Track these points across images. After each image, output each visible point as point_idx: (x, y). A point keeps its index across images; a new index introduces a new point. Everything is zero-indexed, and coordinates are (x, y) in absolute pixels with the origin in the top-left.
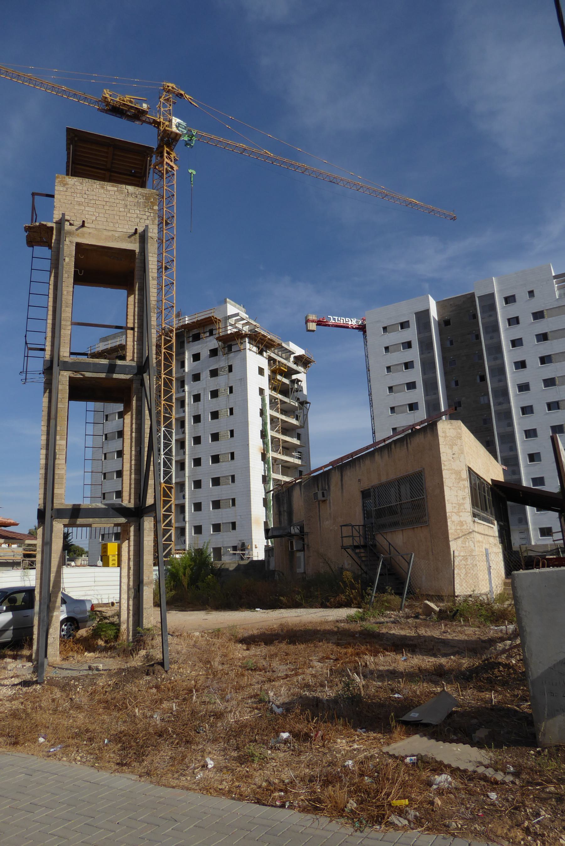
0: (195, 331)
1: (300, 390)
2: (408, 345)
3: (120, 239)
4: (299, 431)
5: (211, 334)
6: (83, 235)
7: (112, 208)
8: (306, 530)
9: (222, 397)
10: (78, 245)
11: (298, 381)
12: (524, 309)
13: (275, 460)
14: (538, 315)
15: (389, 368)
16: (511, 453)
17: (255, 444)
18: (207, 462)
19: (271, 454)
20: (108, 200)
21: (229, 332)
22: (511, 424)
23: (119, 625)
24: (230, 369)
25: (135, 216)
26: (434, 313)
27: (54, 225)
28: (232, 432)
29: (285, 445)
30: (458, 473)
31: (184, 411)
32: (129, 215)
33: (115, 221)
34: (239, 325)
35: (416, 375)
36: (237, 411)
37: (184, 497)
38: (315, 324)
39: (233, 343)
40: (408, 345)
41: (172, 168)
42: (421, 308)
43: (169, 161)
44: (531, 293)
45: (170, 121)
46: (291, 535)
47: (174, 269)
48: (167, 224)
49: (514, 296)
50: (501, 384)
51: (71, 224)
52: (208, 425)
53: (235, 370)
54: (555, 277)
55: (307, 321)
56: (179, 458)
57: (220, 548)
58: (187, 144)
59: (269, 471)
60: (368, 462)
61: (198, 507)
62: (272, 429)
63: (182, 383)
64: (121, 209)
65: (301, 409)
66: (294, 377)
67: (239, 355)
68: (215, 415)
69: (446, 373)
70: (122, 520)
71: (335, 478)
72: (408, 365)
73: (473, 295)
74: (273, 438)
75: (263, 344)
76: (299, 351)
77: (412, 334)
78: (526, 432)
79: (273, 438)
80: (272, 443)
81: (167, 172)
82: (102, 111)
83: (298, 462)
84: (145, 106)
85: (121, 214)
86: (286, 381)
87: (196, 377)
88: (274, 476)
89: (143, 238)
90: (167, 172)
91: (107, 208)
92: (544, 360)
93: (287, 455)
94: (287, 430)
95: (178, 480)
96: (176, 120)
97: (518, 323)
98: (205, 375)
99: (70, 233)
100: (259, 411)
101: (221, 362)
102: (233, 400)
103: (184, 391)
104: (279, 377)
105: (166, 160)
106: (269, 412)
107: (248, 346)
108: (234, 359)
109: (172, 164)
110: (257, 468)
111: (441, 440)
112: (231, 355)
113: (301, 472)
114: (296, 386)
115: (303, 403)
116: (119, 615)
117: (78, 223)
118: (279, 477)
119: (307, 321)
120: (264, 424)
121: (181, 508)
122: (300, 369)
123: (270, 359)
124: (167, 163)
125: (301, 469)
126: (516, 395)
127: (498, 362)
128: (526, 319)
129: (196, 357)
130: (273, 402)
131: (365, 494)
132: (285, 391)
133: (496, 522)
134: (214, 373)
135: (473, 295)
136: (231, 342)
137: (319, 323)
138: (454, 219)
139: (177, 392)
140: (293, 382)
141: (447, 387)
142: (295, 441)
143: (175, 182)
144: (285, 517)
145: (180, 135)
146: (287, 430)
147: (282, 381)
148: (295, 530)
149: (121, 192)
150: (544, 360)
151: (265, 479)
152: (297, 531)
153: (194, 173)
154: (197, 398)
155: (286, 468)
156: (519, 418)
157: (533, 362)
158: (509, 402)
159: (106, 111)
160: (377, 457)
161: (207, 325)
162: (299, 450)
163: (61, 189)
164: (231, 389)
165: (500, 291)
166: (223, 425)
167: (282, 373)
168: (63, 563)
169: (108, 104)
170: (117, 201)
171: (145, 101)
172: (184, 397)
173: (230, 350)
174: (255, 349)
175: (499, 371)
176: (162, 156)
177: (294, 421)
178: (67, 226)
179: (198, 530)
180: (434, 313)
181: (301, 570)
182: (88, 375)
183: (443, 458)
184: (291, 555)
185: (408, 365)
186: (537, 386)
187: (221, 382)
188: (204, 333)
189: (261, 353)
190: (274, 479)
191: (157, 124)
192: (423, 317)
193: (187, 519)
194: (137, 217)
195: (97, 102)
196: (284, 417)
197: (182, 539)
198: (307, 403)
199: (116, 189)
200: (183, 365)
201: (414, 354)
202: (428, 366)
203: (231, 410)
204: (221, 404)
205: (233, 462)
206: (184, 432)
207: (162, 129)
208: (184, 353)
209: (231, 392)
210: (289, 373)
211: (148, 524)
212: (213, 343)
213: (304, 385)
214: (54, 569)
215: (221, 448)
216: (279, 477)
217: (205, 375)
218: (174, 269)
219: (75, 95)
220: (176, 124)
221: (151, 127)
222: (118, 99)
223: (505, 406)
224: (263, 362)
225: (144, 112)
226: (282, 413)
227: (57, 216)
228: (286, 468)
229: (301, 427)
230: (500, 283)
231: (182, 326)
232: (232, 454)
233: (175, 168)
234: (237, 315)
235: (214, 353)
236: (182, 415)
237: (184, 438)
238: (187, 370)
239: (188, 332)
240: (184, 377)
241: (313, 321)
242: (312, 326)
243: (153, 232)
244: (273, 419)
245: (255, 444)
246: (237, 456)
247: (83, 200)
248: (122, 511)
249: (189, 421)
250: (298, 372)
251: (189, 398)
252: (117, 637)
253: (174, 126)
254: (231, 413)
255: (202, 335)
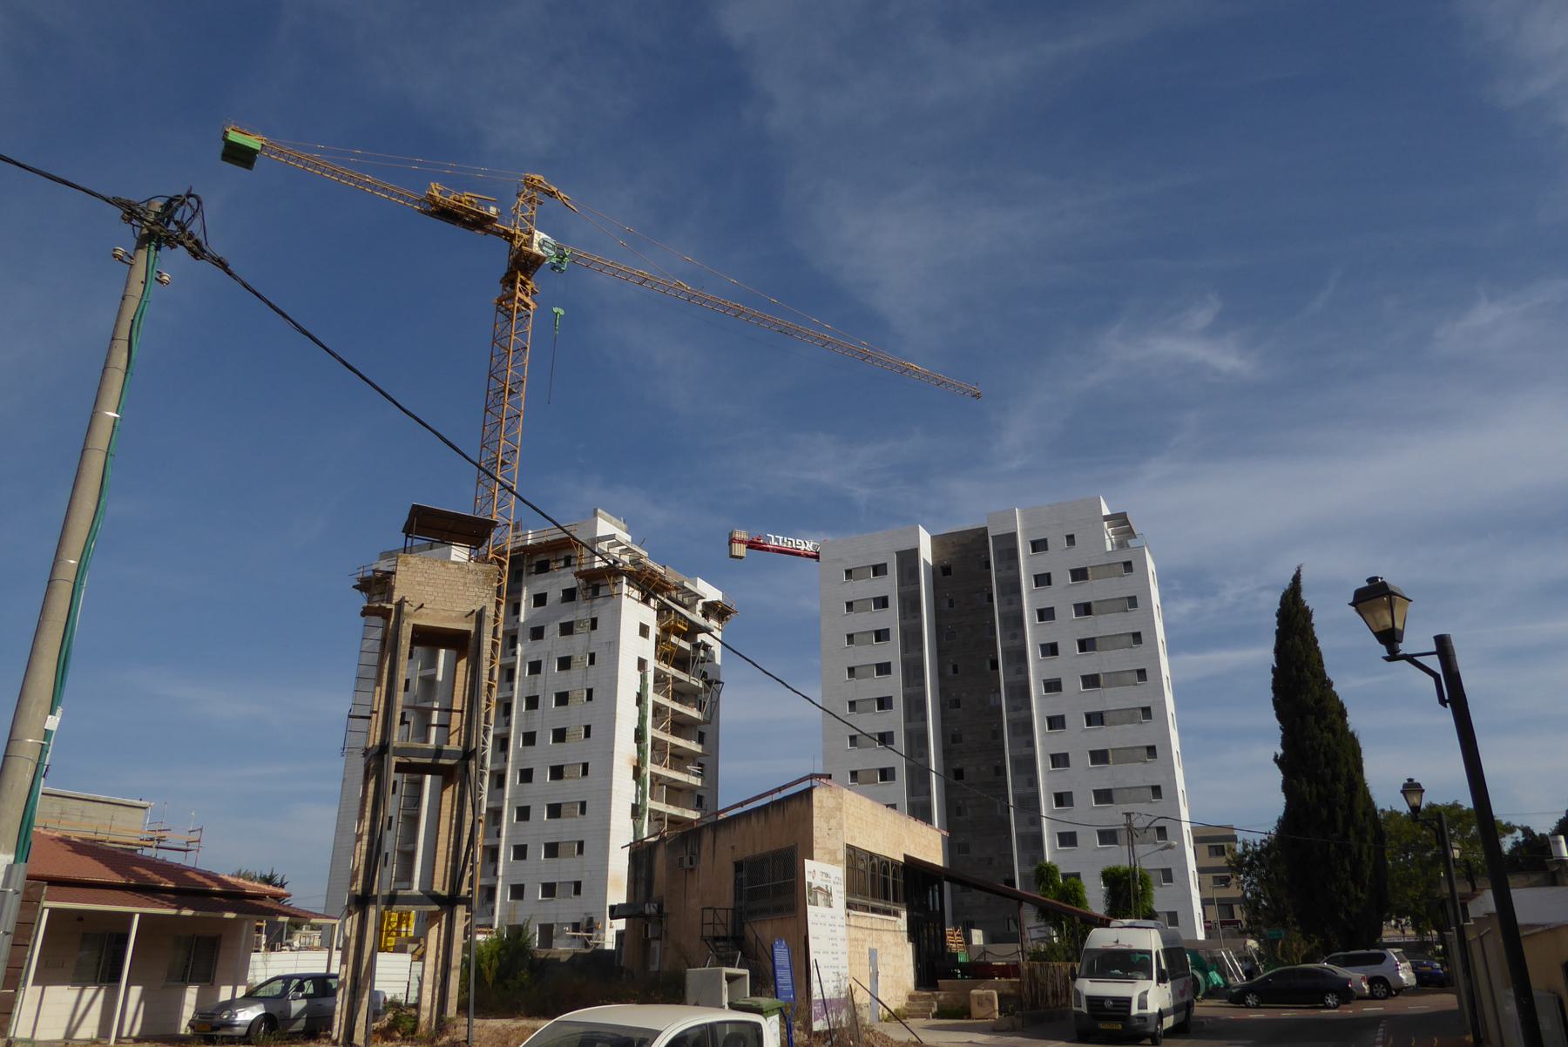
0: (542, 557)
1: (711, 659)
2: (882, 602)
3: (457, 619)
4: (702, 728)
5: (568, 564)
6: (420, 616)
8: (665, 910)
9: (576, 671)
10: (415, 627)
11: (706, 647)
12: (1058, 562)
13: (656, 778)
14: (1079, 575)
15: (850, 637)
16: (1030, 790)
17: (624, 749)
18: (543, 776)
19: (650, 768)
21: (597, 565)
22: (1031, 744)
23: (417, 1018)
24: (594, 624)
26: (926, 554)
27: (392, 606)
28: (588, 729)
29: (676, 751)
30: (833, 853)
31: (512, 688)
34: (615, 551)
35: (892, 652)
36: (600, 695)
37: (498, 835)
38: (744, 547)
39: (601, 582)
40: (882, 602)
41: (527, 306)
42: (906, 546)
43: (523, 297)
44: (1071, 539)
45: (530, 233)
46: (642, 915)
47: (516, 465)
48: (511, 392)
49: (1045, 541)
50: (1020, 677)
52: (549, 716)
53: (603, 628)
54: (1107, 518)
55: (732, 541)
56: (497, 767)
57: (551, 927)
58: (554, 267)
59: (644, 797)
60: (743, 824)
61: (520, 852)
62: (655, 726)
63: (512, 640)
65: (707, 691)
66: (701, 637)
67: (613, 602)
68: (562, 699)
69: (941, 652)
70: (436, 908)
71: (707, 838)
72: (881, 635)
73: (983, 533)
74: (655, 741)
75: (649, 586)
76: (712, 594)
77: (889, 585)
78: (1053, 757)
79: (655, 741)
80: (653, 748)
81: (519, 310)
82: (426, 213)
83: (696, 781)
84: (493, 210)
86: (686, 646)
87: (537, 633)
88: (651, 804)
89: (480, 617)
90: (519, 310)
92: (1085, 645)
93: (678, 769)
94: (680, 726)
95: (492, 805)
96: (539, 236)
97: (1049, 583)
98: (552, 630)
99: (409, 615)
100: (635, 697)
101: (579, 612)
102: (594, 677)
103: (514, 654)
104: (674, 639)
105: (519, 294)
106: (652, 697)
107: (625, 588)
108: (601, 610)
109: (527, 300)
110: (623, 791)
111: (816, 811)
112: (597, 601)
113: (700, 799)
114: (702, 653)
115: (712, 683)
116: (417, 1006)
117: (416, 605)
118: (661, 807)
119: (732, 541)
120: (642, 719)
121: (492, 853)
122: (713, 623)
123: (662, 610)
124: (520, 301)
125: (700, 793)
126: (1040, 697)
127: (1017, 642)
128: (1062, 578)
129: (540, 600)
130: (660, 679)
131: (738, 866)
132: (681, 661)
133: (904, 914)
134: (567, 629)
135: (985, 530)
136: (599, 583)
137: (752, 545)
138: (977, 396)
139: (504, 655)
140: (697, 646)
141: (941, 674)
142: (694, 746)
143: (529, 328)
144: (642, 888)
145: (544, 259)
146: (680, 726)
147: (679, 648)
148: (650, 909)
150: (1085, 645)
151: (636, 811)
152: (653, 910)
153: (562, 312)
154: (535, 668)
155: (675, 792)
156: (1044, 735)
157: (1069, 647)
158: (1030, 708)
159: (432, 214)
160: (754, 819)
161: (560, 550)
162: (700, 760)
164: (592, 657)
165: (1026, 531)
166: (572, 717)
167: (678, 633)
168: (380, 947)
169: (435, 204)
171: (495, 204)
172: (514, 664)
173: (596, 593)
174: (636, 594)
175: (1018, 657)
176: (513, 287)
177: (694, 713)
178: (407, 608)
179: (518, 892)
180: (926, 554)
181: (654, 968)
182: (414, 760)
183: (816, 833)
184: (646, 943)
185: (881, 635)
186: (1073, 685)
187: (576, 645)
188: (557, 561)
189: (646, 601)
190: (651, 811)
191: (510, 237)
192: (909, 559)
193: (500, 872)
195: (419, 202)
196: (677, 706)
197: (489, 906)
198: (718, 682)
200: (516, 609)
201: (891, 619)
202: (911, 638)
203: (590, 692)
204: (573, 682)
205: (586, 779)
206: (508, 724)
207: (516, 244)
208: (520, 592)
209: (592, 662)
210: (693, 630)
211: (461, 912)
212: (568, 579)
213: (717, 648)
214: (367, 955)
215: (567, 754)
216: (661, 807)
217: (552, 630)
218: (516, 465)
219: (384, 190)
220: (539, 241)
221: (501, 240)
222: (450, 199)
223: (1023, 713)
224: (649, 615)
225: (490, 220)
226: (674, 699)
227: (396, 598)
228: (675, 792)
229: (705, 722)
230: (1025, 518)
231: (521, 548)
232: (585, 766)
233: (532, 306)
234: (612, 537)
235: (569, 595)
236: (508, 694)
237: (508, 734)
238: (522, 619)
239: (531, 557)
240: (516, 630)
241: (741, 542)
242: (740, 550)
243: (490, 612)
244: (658, 709)
245: (624, 749)
246: (594, 770)
248: (436, 898)
249: (520, 705)
250: (708, 631)
251: (523, 666)
252: (414, 1031)
253: (535, 245)
254: (590, 698)
255: (552, 565)
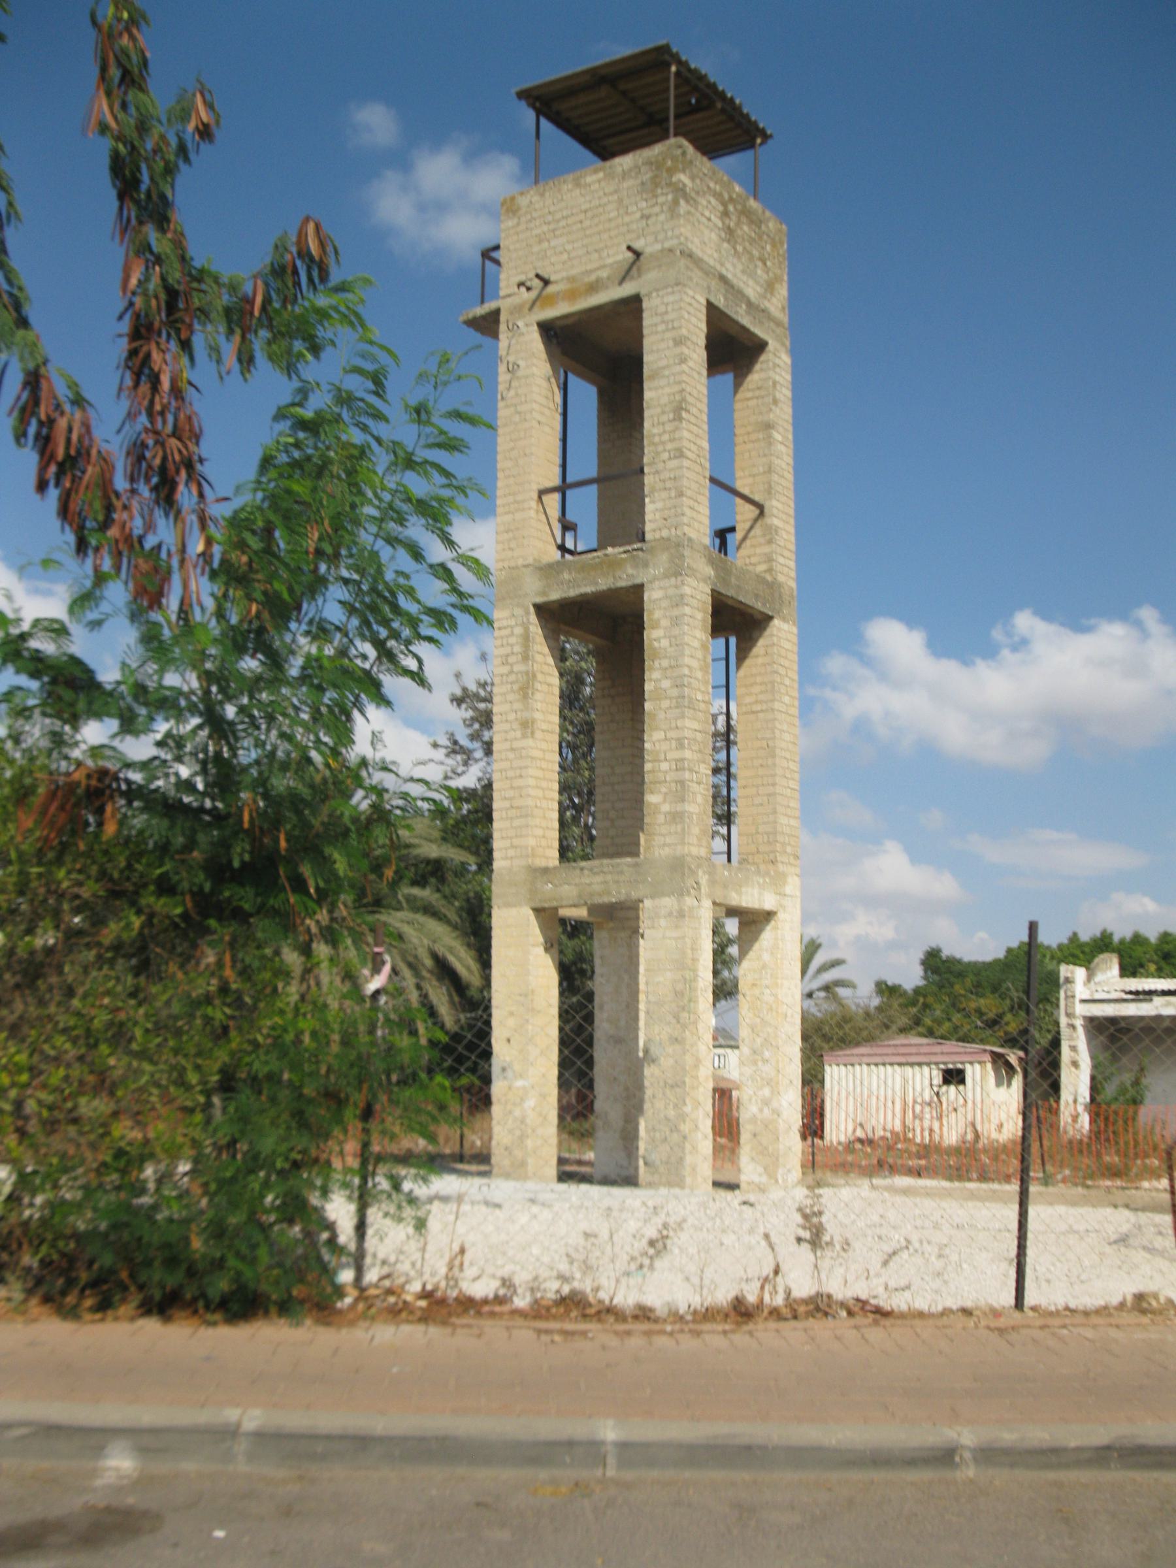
7: (596, 220)
20: (587, 206)
25: (638, 215)
32: (627, 219)
33: (602, 245)
51: (528, 289)
64: (614, 214)
85: (613, 224)
91: (587, 223)
149: (610, 176)
163: (510, 223)
170: (605, 200)
194: (642, 217)
199: (601, 175)
247: (545, 228)
